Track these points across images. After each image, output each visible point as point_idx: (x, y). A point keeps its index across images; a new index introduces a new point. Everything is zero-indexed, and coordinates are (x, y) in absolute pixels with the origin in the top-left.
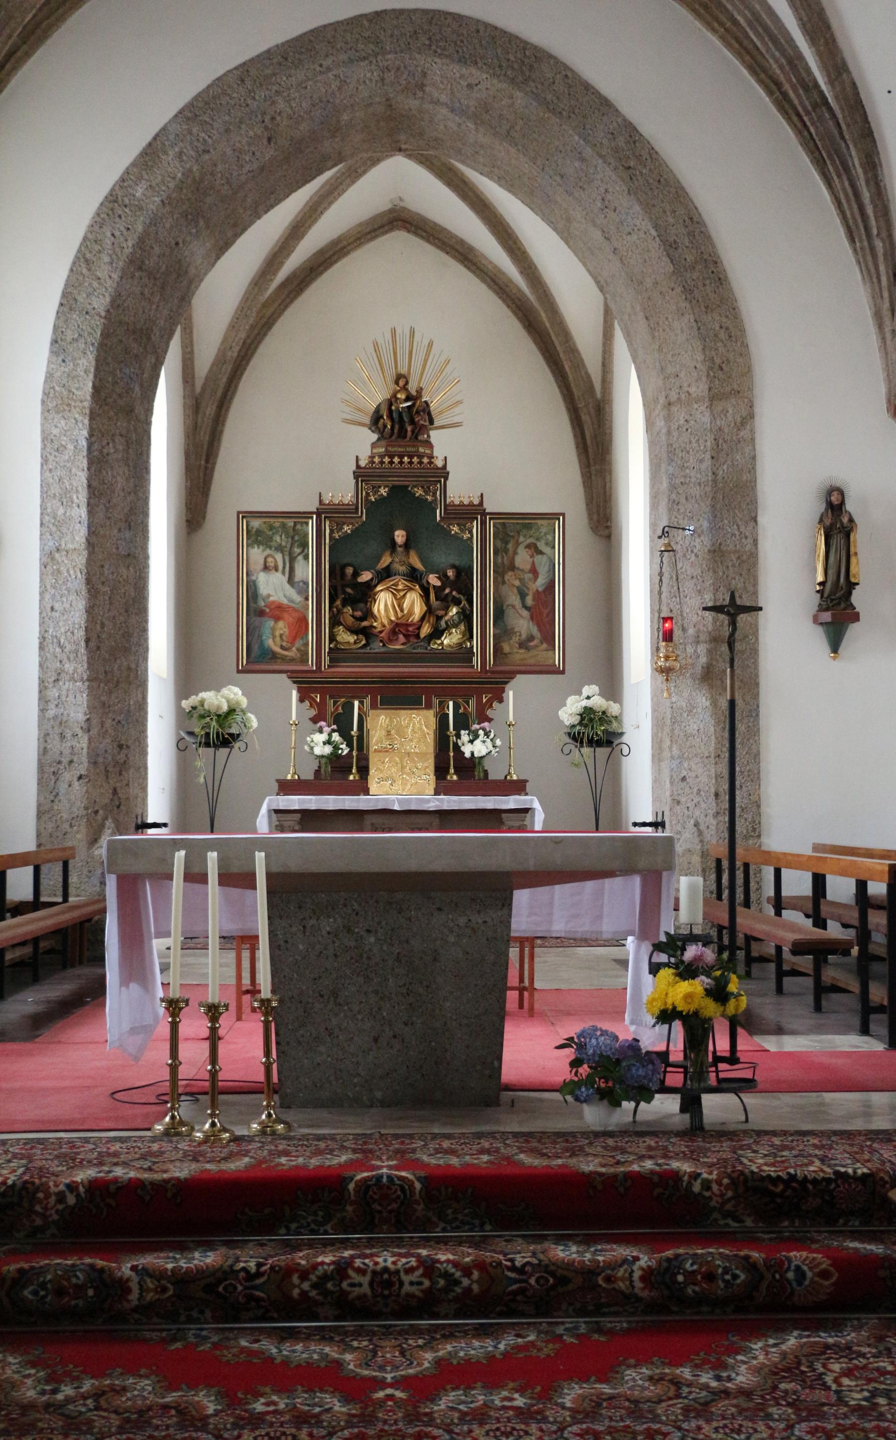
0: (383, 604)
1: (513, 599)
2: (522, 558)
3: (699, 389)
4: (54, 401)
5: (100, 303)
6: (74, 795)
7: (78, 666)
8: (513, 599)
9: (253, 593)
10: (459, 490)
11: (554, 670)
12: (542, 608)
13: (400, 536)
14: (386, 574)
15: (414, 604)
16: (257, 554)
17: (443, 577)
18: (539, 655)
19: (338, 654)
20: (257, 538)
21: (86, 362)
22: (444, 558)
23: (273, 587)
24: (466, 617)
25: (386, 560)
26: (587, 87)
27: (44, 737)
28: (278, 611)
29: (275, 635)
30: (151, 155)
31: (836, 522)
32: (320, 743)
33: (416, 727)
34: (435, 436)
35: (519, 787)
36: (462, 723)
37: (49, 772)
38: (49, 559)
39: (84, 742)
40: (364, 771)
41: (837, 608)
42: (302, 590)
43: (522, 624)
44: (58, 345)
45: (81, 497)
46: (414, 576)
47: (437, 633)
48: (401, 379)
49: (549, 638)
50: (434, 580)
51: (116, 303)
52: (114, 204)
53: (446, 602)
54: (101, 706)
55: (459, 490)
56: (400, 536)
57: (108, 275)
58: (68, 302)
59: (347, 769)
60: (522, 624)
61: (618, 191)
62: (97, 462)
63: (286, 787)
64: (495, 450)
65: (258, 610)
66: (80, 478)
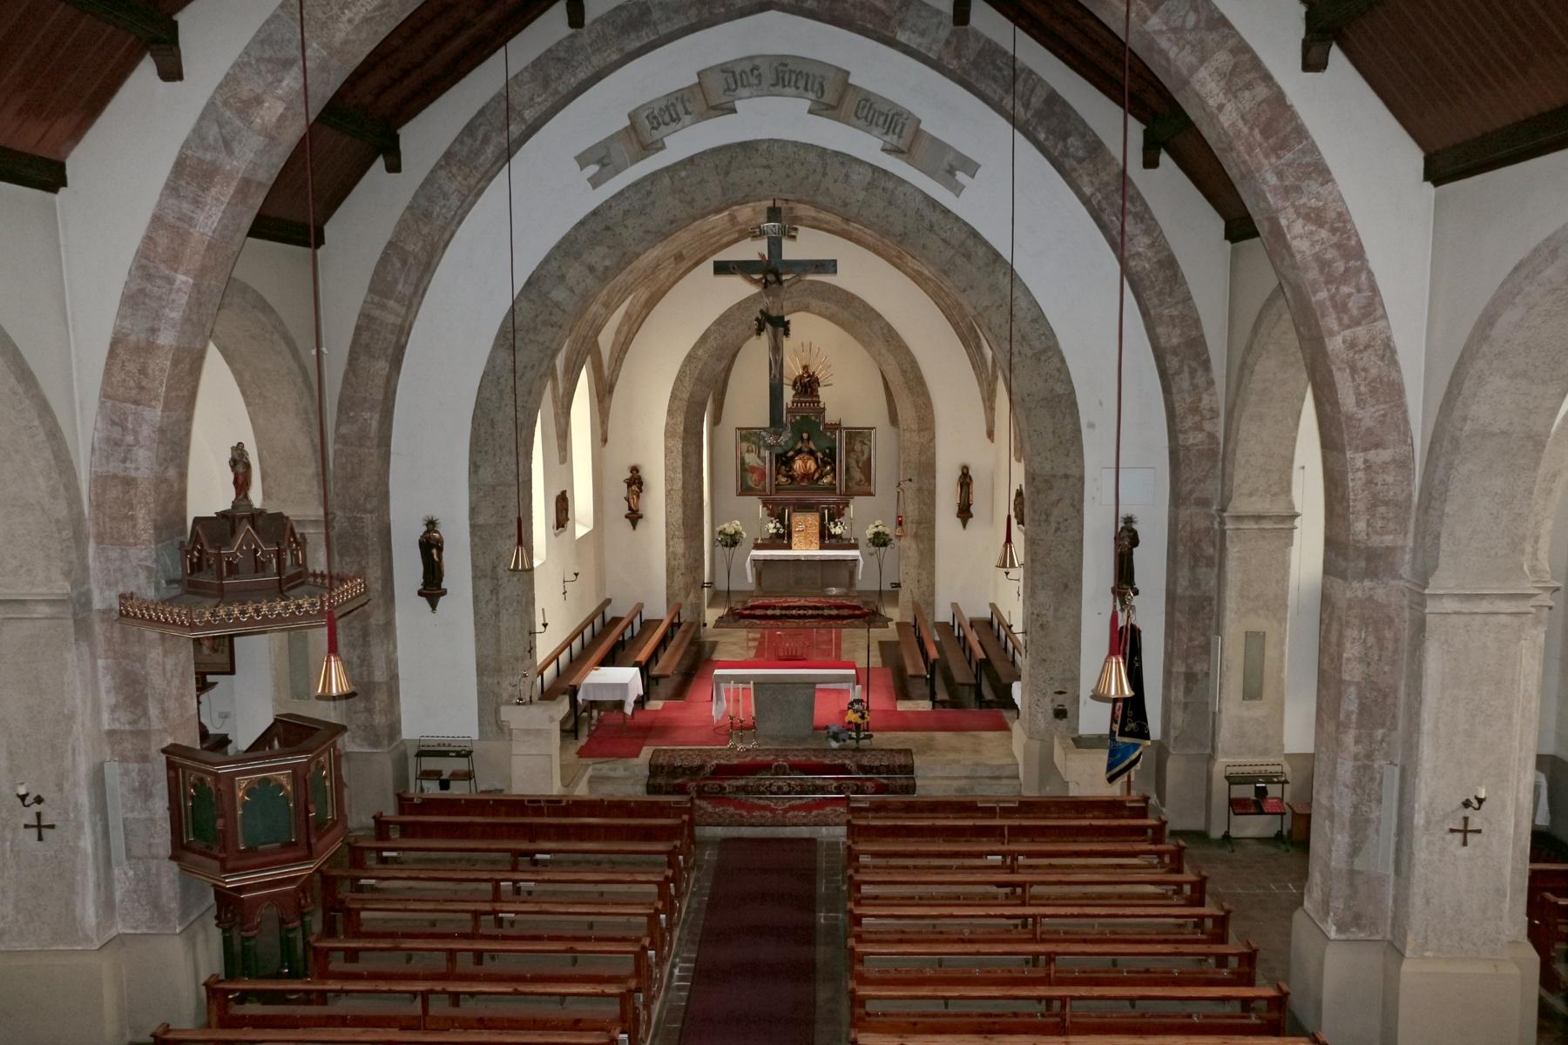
0: (798, 464)
1: (853, 464)
2: (858, 447)
3: (915, 427)
4: (669, 433)
5: (686, 396)
6: (680, 581)
7: (680, 533)
8: (853, 464)
9: (743, 460)
10: (830, 417)
11: (870, 494)
12: (867, 468)
13: (805, 436)
14: (799, 452)
15: (811, 465)
16: (745, 445)
17: (824, 454)
18: (865, 488)
19: (779, 488)
20: (744, 438)
21: (681, 419)
22: (825, 444)
23: (751, 459)
24: (834, 470)
25: (799, 445)
26: (872, 309)
27: (668, 560)
28: (753, 469)
29: (752, 480)
30: (704, 338)
31: (965, 480)
32: (771, 527)
33: (812, 520)
34: (821, 391)
35: (855, 547)
36: (831, 518)
37: (670, 572)
38: (668, 494)
39: (682, 562)
40: (790, 537)
41: (964, 513)
42: (763, 460)
43: (857, 475)
44: (671, 413)
45: (680, 470)
46: (812, 453)
47: (821, 477)
48: (805, 368)
49: (869, 480)
50: (820, 455)
51: (692, 395)
52: (690, 358)
53: (825, 464)
54: (688, 548)
55: (830, 417)
56: (805, 436)
57: (688, 385)
58: (673, 397)
59: (782, 539)
60: (857, 475)
61: (884, 351)
62: (685, 456)
63: (757, 547)
64: (850, 396)
65: (744, 469)
66: (680, 463)
